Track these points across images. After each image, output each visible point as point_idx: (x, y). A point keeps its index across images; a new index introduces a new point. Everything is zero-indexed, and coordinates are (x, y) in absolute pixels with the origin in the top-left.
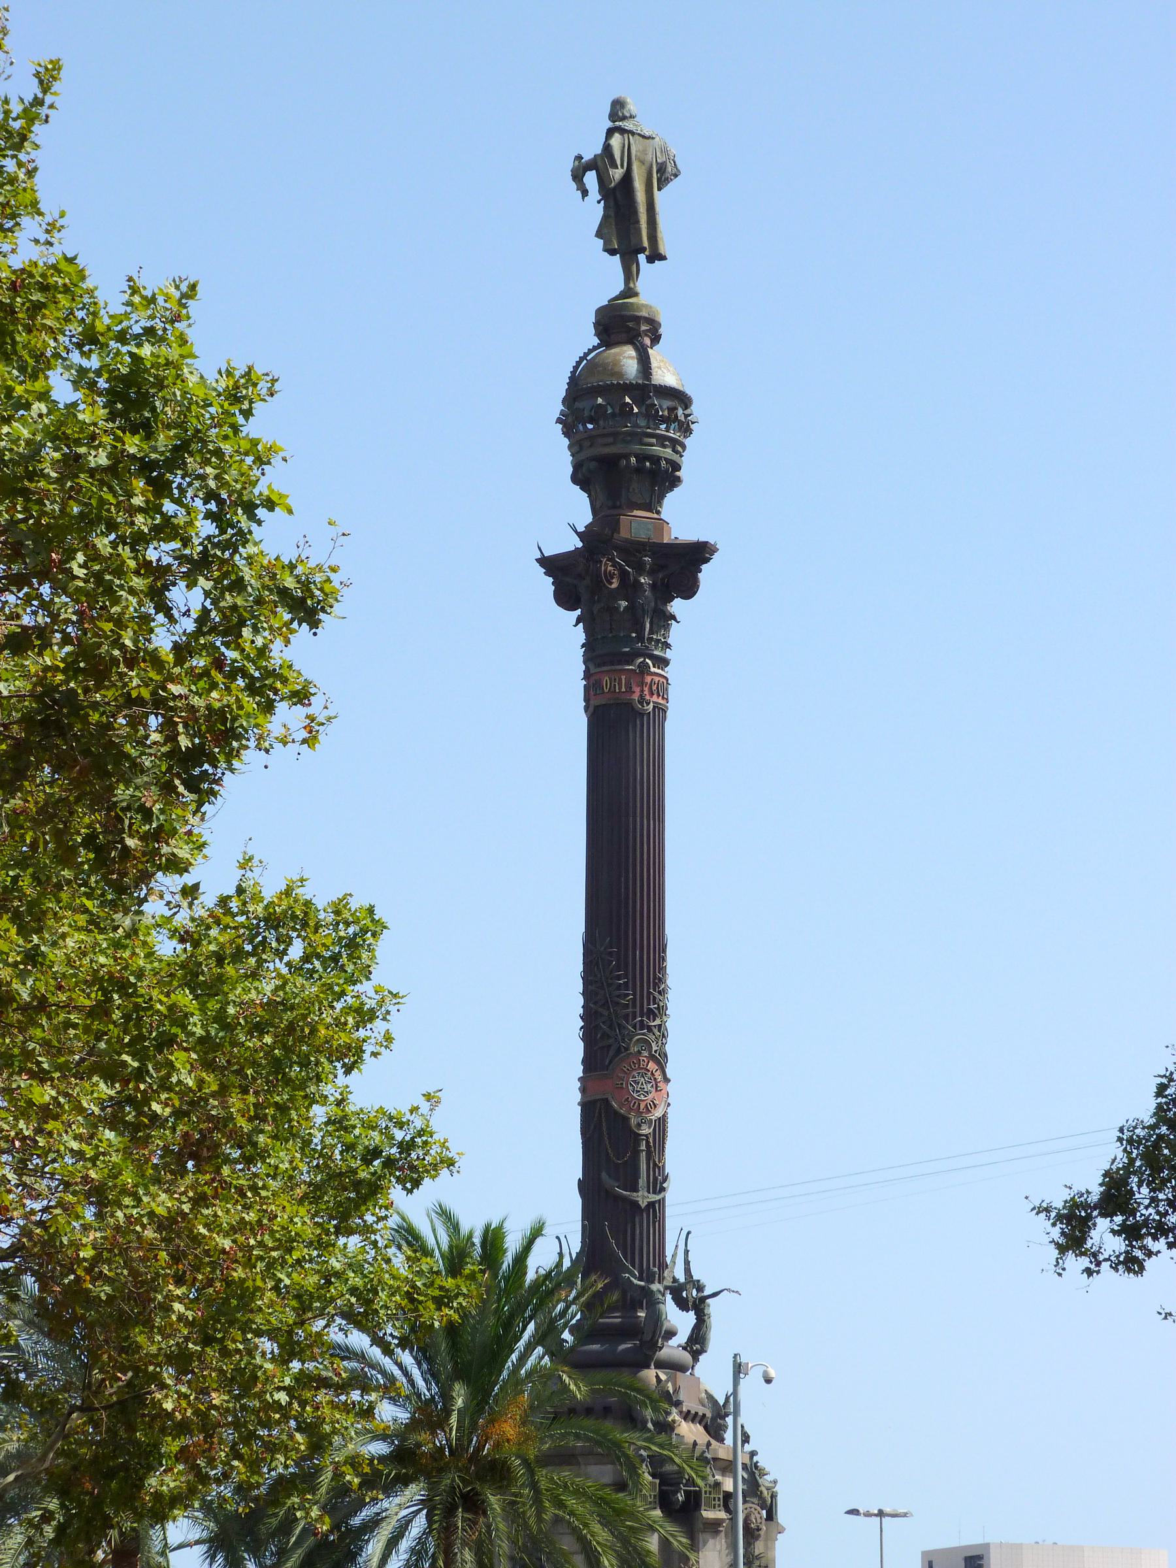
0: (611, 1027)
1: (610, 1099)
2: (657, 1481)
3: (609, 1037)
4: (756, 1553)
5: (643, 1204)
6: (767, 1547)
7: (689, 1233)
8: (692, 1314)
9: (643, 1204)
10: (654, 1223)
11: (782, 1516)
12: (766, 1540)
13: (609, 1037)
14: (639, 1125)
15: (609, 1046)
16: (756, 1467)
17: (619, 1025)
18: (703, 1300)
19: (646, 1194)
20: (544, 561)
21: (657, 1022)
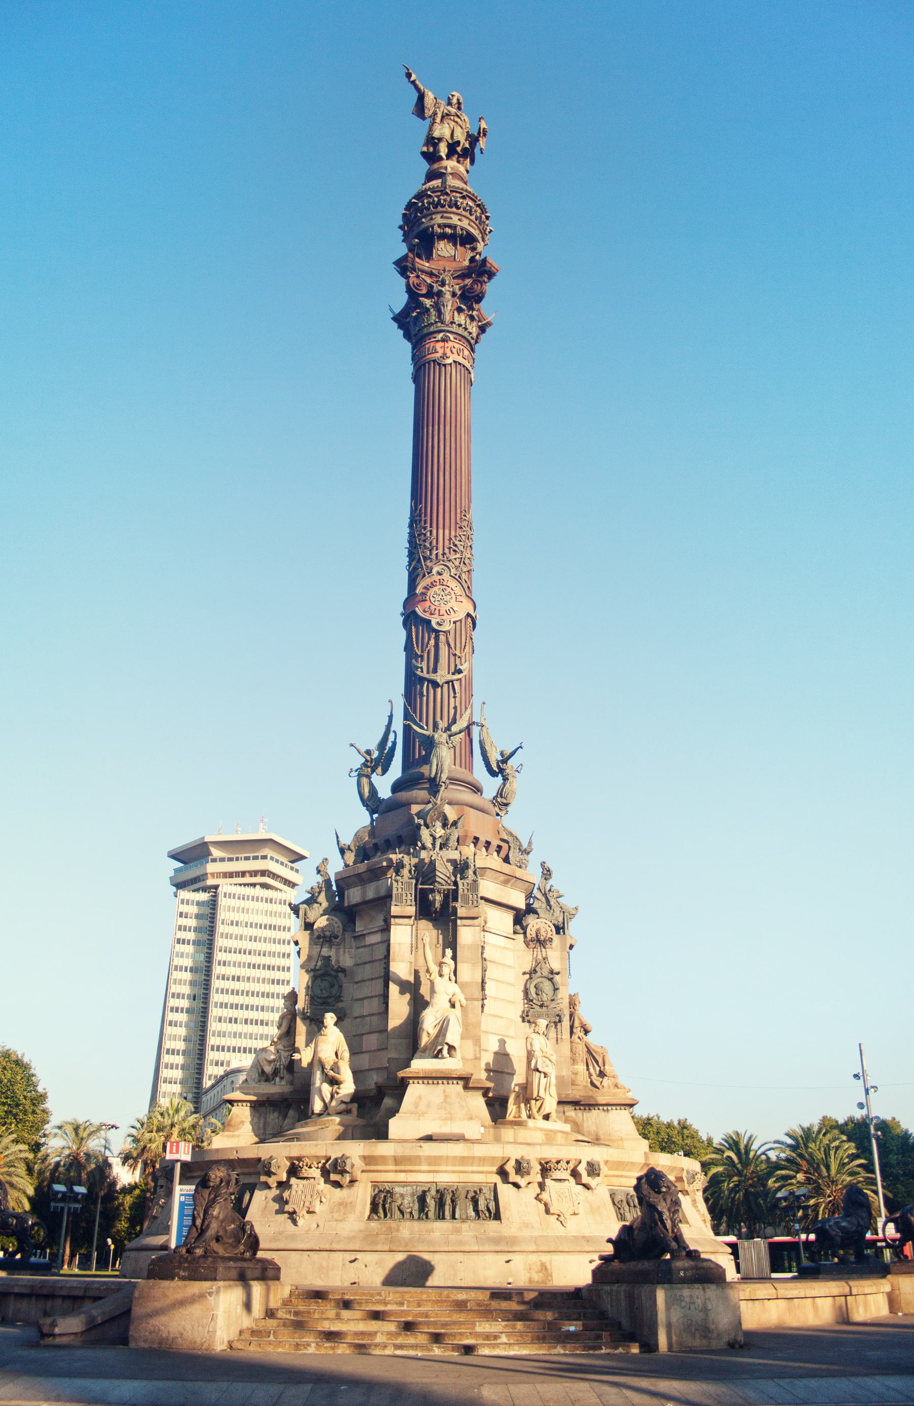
9: (440, 681)
10: (455, 697)
15: (418, 576)
18: (505, 761)
20: (395, 319)
21: (458, 556)
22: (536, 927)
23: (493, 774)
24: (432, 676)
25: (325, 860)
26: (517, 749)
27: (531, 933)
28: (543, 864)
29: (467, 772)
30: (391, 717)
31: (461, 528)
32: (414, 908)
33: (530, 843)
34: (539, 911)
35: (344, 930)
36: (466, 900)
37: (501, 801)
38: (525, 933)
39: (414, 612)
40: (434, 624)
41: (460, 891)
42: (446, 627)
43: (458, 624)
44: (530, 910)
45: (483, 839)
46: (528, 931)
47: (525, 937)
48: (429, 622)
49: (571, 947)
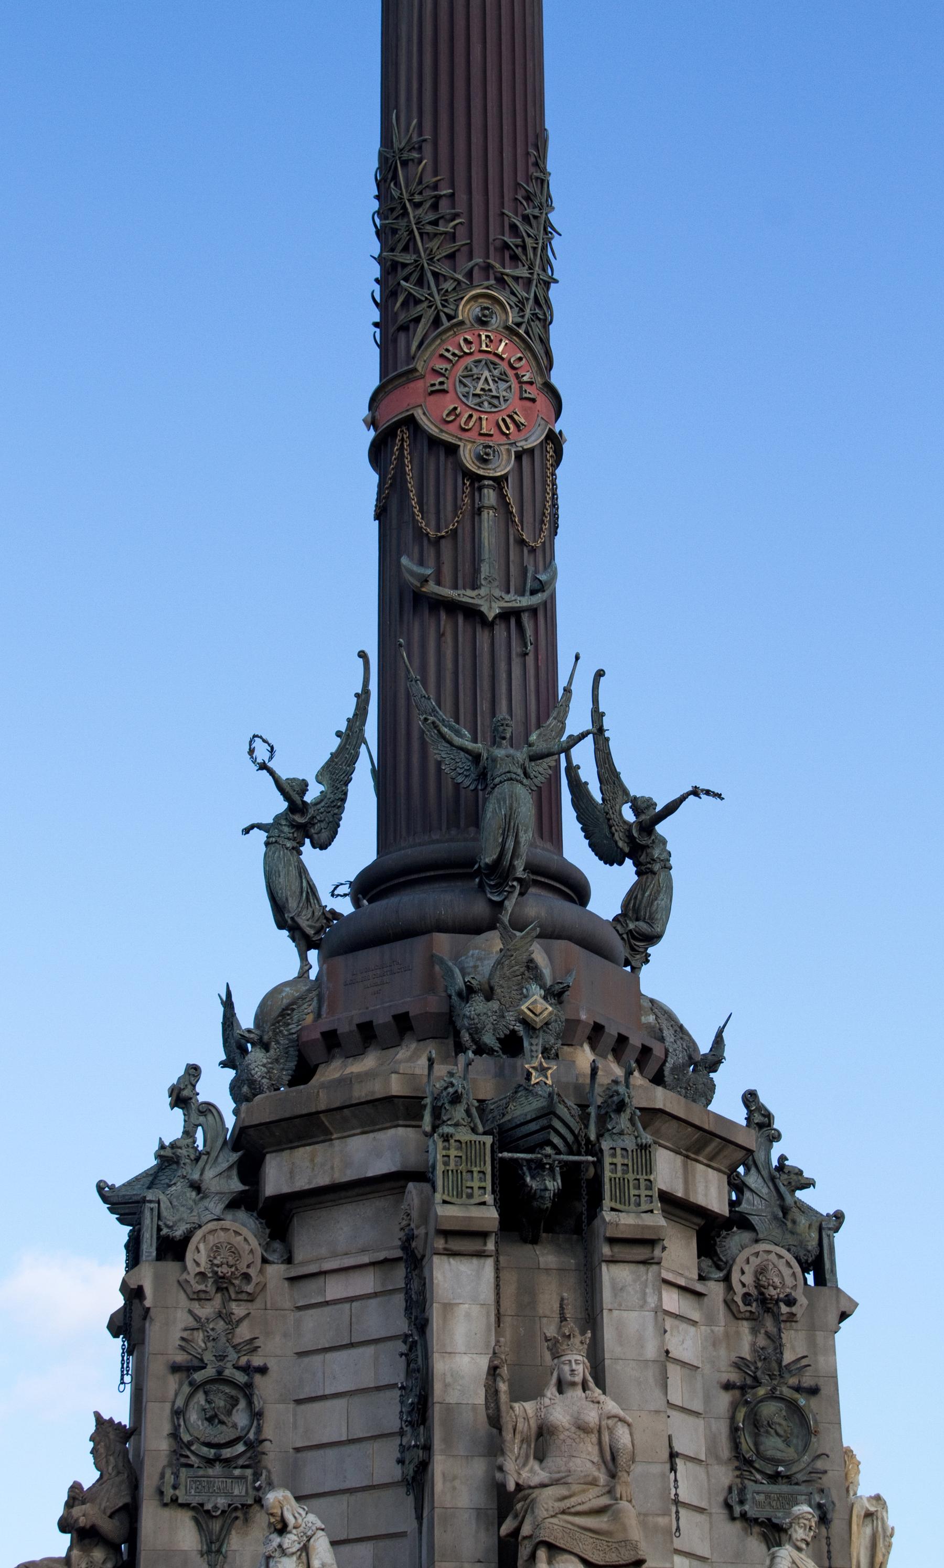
0: (420, 282)
1: (419, 414)
2: (489, 1140)
3: (418, 302)
4: (788, 1357)
5: (491, 611)
6: (812, 1343)
7: (600, 674)
8: (628, 862)
9: (491, 611)
11: (849, 1273)
12: (812, 1328)
13: (418, 302)
14: (483, 460)
15: (417, 320)
16: (781, 1167)
17: (436, 275)
19: (497, 593)
22: (755, 1261)
23: (610, 857)
24: (466, 596)
25: (193, 1072)
26: (683, 798)
27: (743, 1278)
28: (750, 1098)
29: (548, 845)
30: (362, 698)
31: (528, 198)
32: (493, 1213)
33: (719, 1041)
34: (754, 1220)
35: (265, 1261)
36: (622, 1197)
37: (641, 926)
38: (727, 1279)
39: (410, 422)
40: (467, 456)
41: (607, 1167)
42: (503, 466)
43: (525, 460)
44: (739, 1221)
45: (612, 1030)
46: (735, 1277)
47: (730, 1288)
48: (452, 450)
49: (844, 1316)
